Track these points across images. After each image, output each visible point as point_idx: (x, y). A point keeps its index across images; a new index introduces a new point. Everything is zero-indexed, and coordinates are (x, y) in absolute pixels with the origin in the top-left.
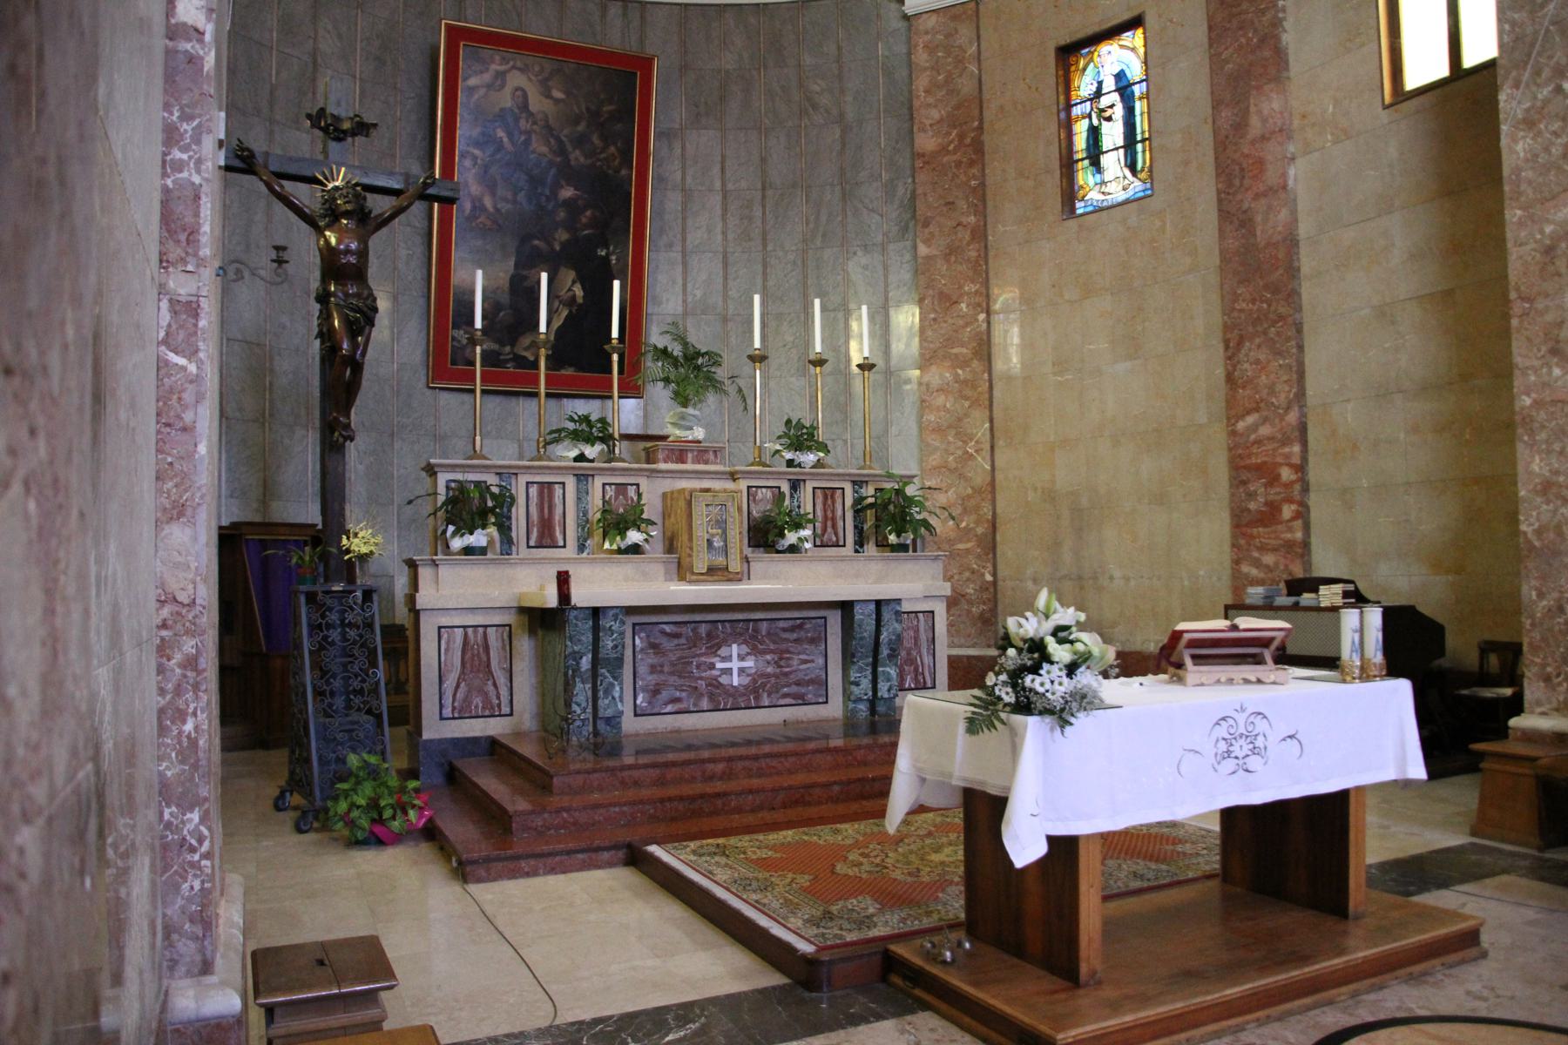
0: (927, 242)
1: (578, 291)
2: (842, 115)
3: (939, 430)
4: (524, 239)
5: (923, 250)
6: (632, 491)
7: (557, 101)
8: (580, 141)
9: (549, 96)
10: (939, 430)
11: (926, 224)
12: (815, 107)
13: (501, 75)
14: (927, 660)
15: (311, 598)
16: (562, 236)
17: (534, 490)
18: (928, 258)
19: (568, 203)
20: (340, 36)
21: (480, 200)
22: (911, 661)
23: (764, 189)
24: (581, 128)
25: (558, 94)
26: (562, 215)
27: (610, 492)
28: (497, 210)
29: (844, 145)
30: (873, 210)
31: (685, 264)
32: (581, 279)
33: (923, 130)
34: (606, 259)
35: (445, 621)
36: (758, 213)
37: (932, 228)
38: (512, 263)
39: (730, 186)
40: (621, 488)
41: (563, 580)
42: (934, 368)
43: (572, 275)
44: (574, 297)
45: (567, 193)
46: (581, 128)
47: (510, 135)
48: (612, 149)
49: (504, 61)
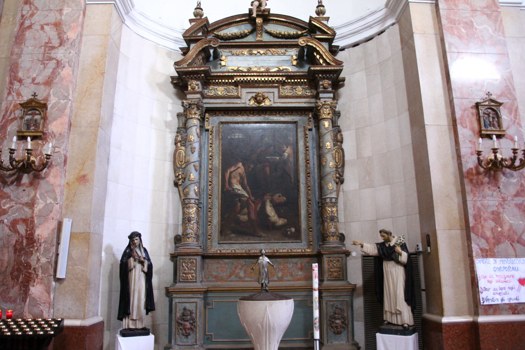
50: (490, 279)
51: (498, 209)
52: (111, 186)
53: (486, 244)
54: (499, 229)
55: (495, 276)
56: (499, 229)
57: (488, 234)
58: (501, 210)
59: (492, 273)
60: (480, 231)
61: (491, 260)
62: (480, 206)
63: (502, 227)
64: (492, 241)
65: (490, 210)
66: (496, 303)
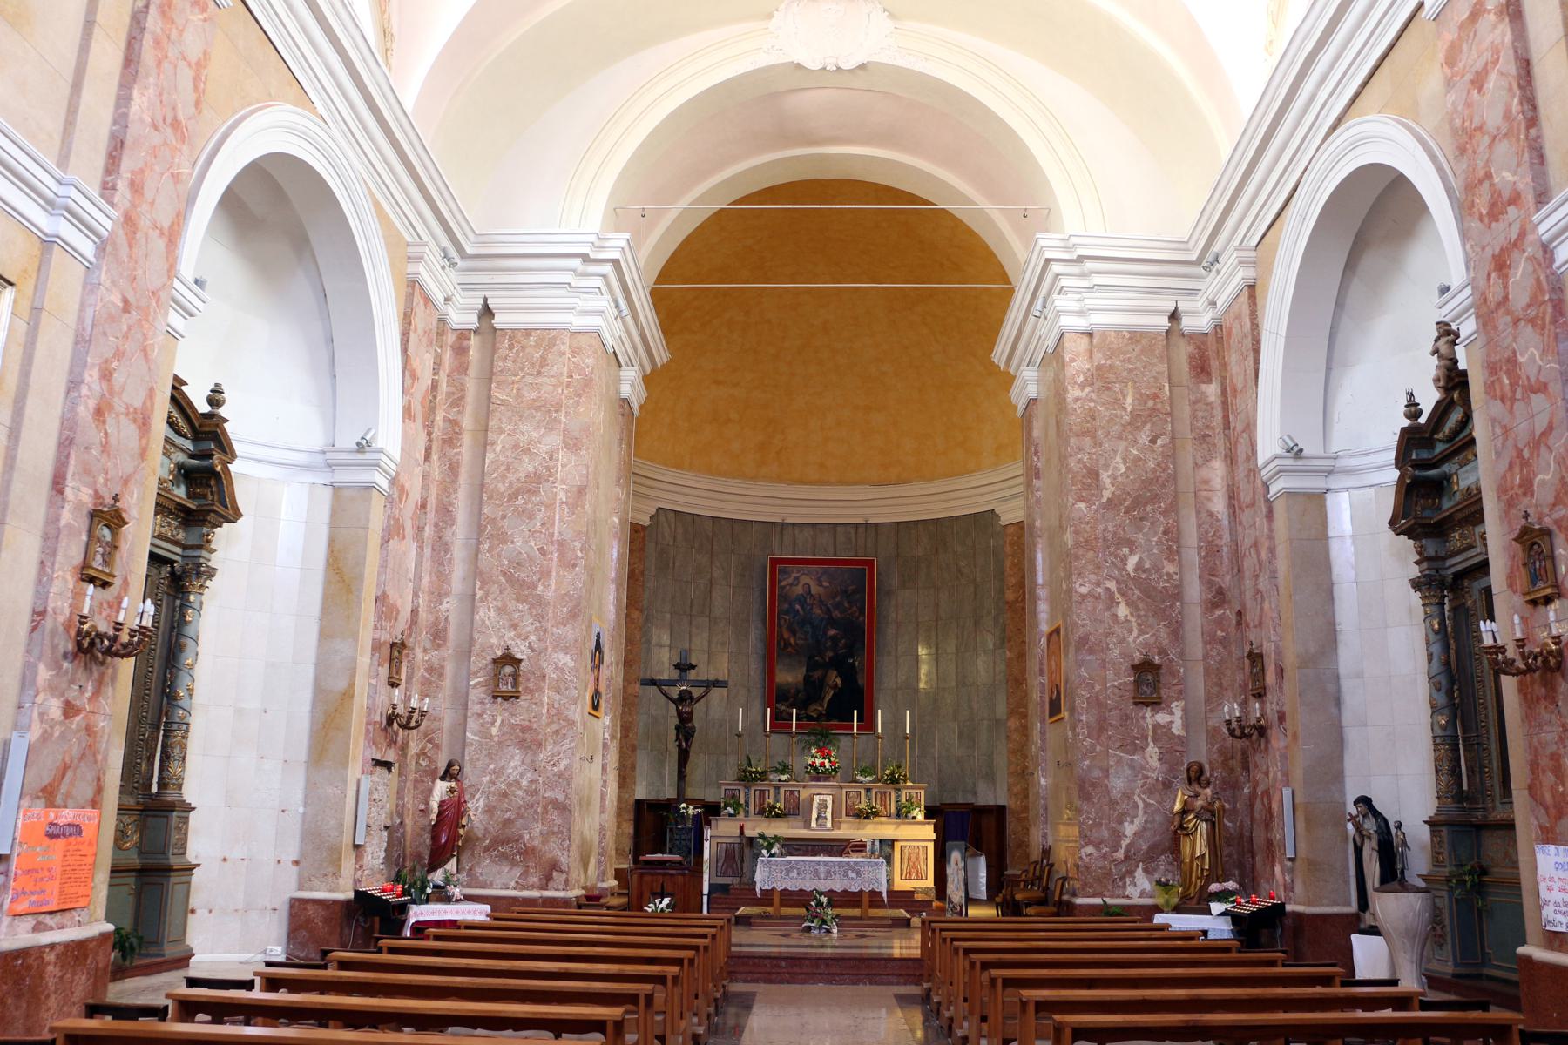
0: (1010, 651)
1: (839, 681)
2: (975, 580)
3: (1013, 752)
4: (810, 658)
5: (1008, 654)
6: (796, 793)
7: (826, 587)
8: (838, 606)
9: (821, 586)
10: (1013, 752)
11: (1009, 641)
12: (962, 574)
13: (797, 579)
14: (923, 867)
15: (671, 830)
16: (830, 654)
17: (757, 793)
18: (1010, 658)
19: (833, 638)
20: (723, 569)
21: (789, 640)
22: (916, 867)
23: (937, 620)
24: (838, 599)
25: (825, 584)
26: (829, 644)
27: (788, 793)
28: (797, 644)
29: (976, 594)
30: (988, 631)
31: (897, 662)
32: (840, 675)
33: (1008, 589)
34: (853, 664)
35: (719, 841)
36: (933, 633)
37: (1012, 643)
38: (804, 669)
39: (920, 620)
40: (792, 792)
41: (742, 828)
42: (1012, 719)
43: (835, 673)
44: (836, 685)
45: (832, 632)
46: (838, 599)
47: (802, 607)
48: (855, 608)
49: (798, 571)
50: (1550, 884)
51: (1558, 748)
52: (1352, 735)
53: (1546, 817)
54: (1561, 789)
55: (1556, 879)
56: (1561, 789)
57: (1548, 797)
58: (1562, 751)
59: (1554, 873)
60: (1539, 792)
61: (1552, 848)
62: (1536, 744)
63: (1563, 786)
64: (1553, 811)
65: (1549, 751)
66: (1558, 929)
